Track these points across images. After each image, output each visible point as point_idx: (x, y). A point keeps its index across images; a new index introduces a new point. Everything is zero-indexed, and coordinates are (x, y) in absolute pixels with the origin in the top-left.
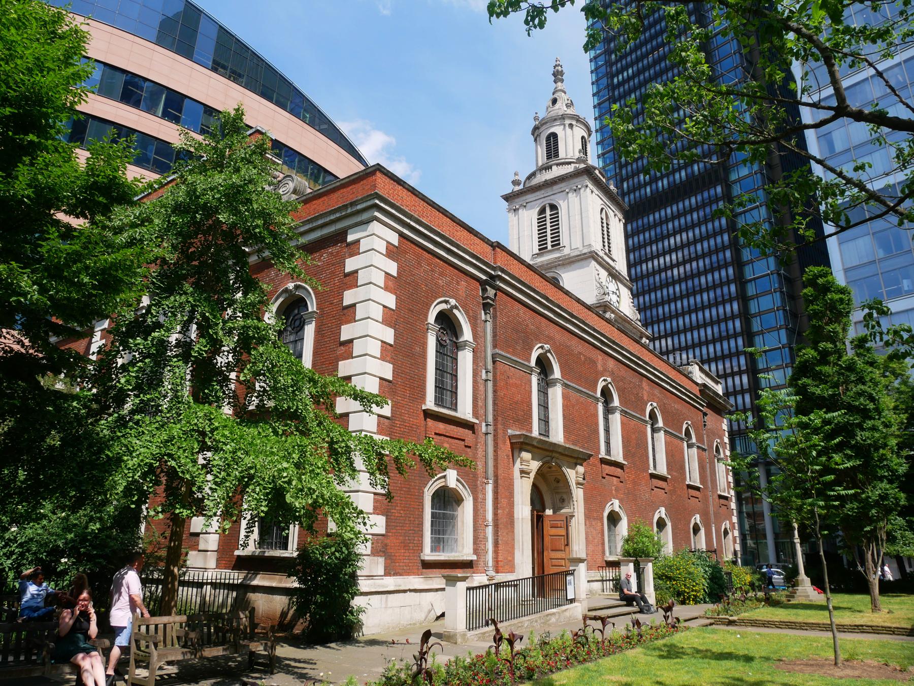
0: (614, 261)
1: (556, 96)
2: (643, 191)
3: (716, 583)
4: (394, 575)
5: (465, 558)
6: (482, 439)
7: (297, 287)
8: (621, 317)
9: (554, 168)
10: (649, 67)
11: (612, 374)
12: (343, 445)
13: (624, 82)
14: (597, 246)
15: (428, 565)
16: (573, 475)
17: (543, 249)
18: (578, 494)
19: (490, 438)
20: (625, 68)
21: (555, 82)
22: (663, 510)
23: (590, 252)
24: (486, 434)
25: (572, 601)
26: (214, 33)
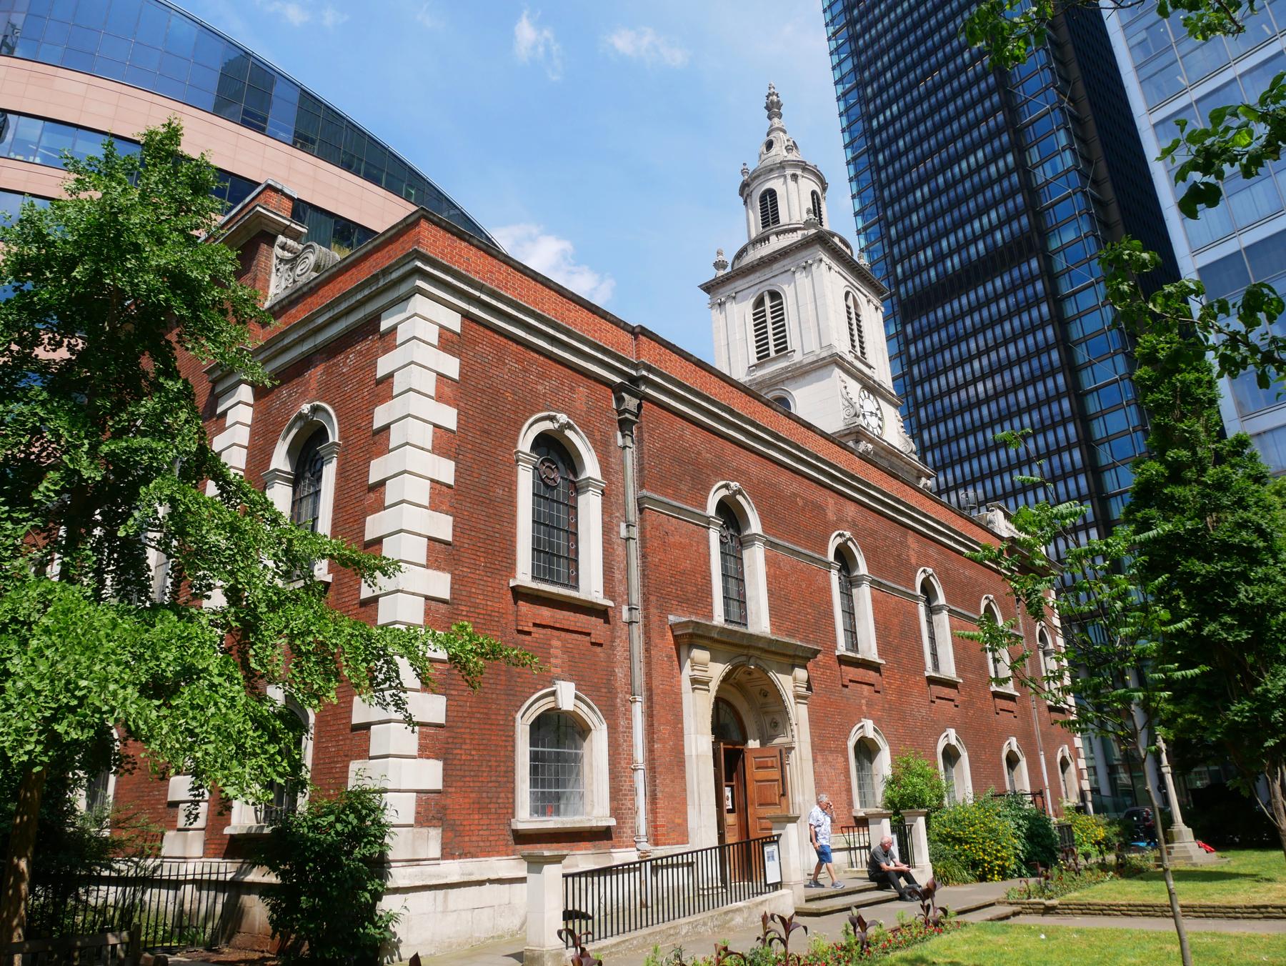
0: (870, 367)
1: (771, 137)
2: (925, 276)
3: (1039, 844)
4: (460, 857)
5: (600, 824)
6: (622, 632)
7: (315, 410)
8: (884, 448)
9: (773, 238)
10: (920, 100)
11: (853, 526)
12: (310, 639)
14: (842, 346)
15: (523, 838)
16: (788, 684)
17: (763, 356)
18: (799, 714)
19: (637, 631)
20: (888, 105)
21: (770, 118)
22: (952, 732)
23: (831, 356)
24: (630, 623)
25: (777, 886)
26: (295, 97)
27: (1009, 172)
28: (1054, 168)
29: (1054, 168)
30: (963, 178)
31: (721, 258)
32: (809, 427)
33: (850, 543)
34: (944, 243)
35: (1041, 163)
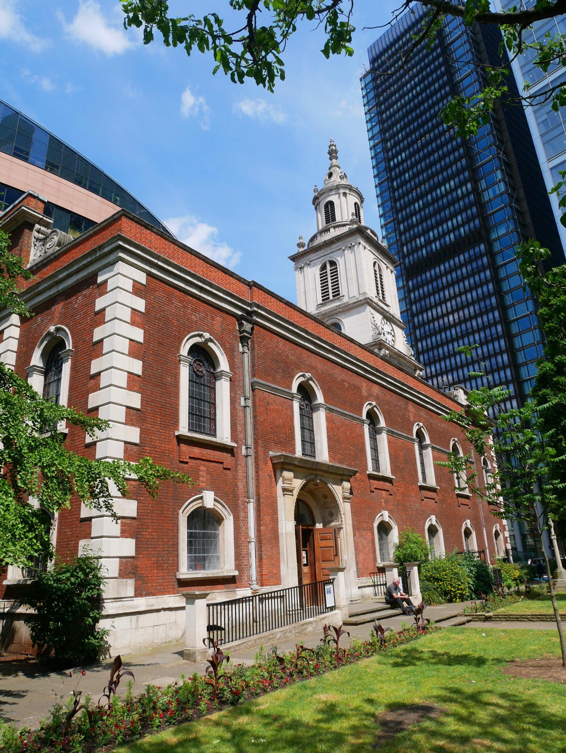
0: (388, 306)
1: (331, 170)
2: (420, 253)
3: (482, 581)
4: (146, 595)
5: (229, 574)
6: (242, 461)
7: (58, 330)
8: (395, 353)
9: (332, 230)
11: (377, 399)
12: (54, 469)
13: (399, 164)
14: (372, 293)
15: (183, 583)
16: (339, 491)
17: (326, 299)
18: (345, 508)
19: (251, 461)
20: (400, 153)
21: (331, 159)
22: (433, 517)
23: (365, 299)
24: (247, 456)
25: (332, 608)
26: (47, 140)
27: (468, 194)
28: (494, 192)
29: (494, 192)
30: (442, 196)
31: (301, 241)
32: (352, 341)
33: (375, 409)
34: (431, 234)
35: (487, 189)
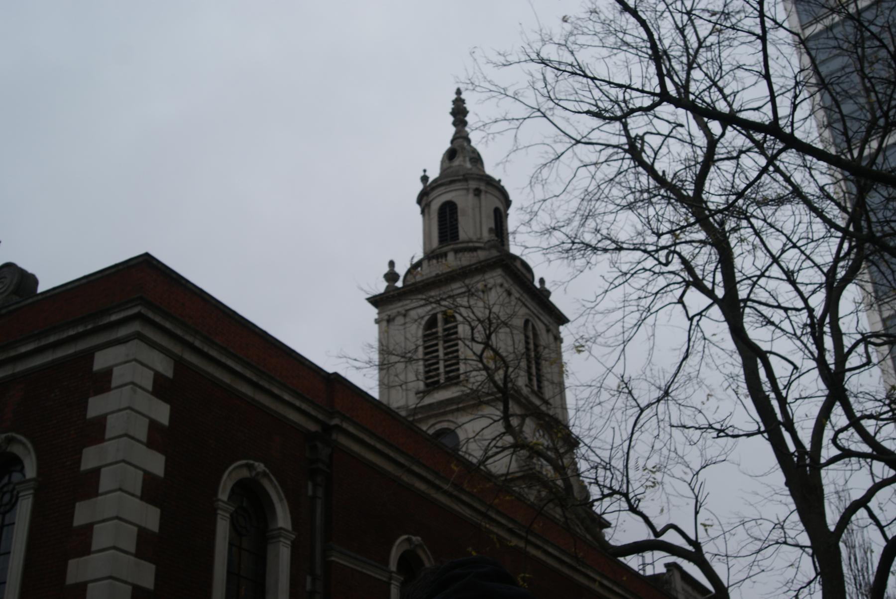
0: (546, 402)
9: (451, 256)
